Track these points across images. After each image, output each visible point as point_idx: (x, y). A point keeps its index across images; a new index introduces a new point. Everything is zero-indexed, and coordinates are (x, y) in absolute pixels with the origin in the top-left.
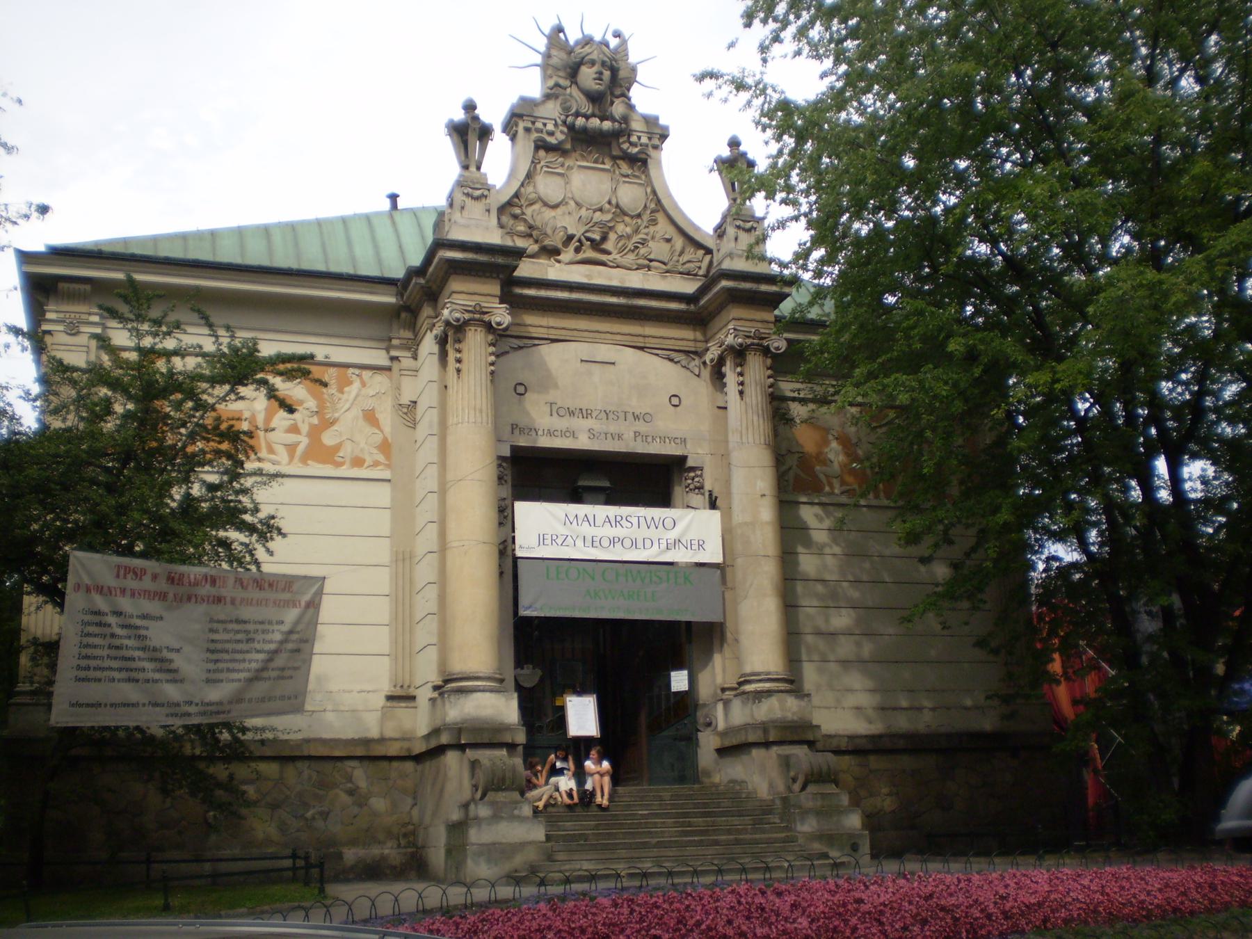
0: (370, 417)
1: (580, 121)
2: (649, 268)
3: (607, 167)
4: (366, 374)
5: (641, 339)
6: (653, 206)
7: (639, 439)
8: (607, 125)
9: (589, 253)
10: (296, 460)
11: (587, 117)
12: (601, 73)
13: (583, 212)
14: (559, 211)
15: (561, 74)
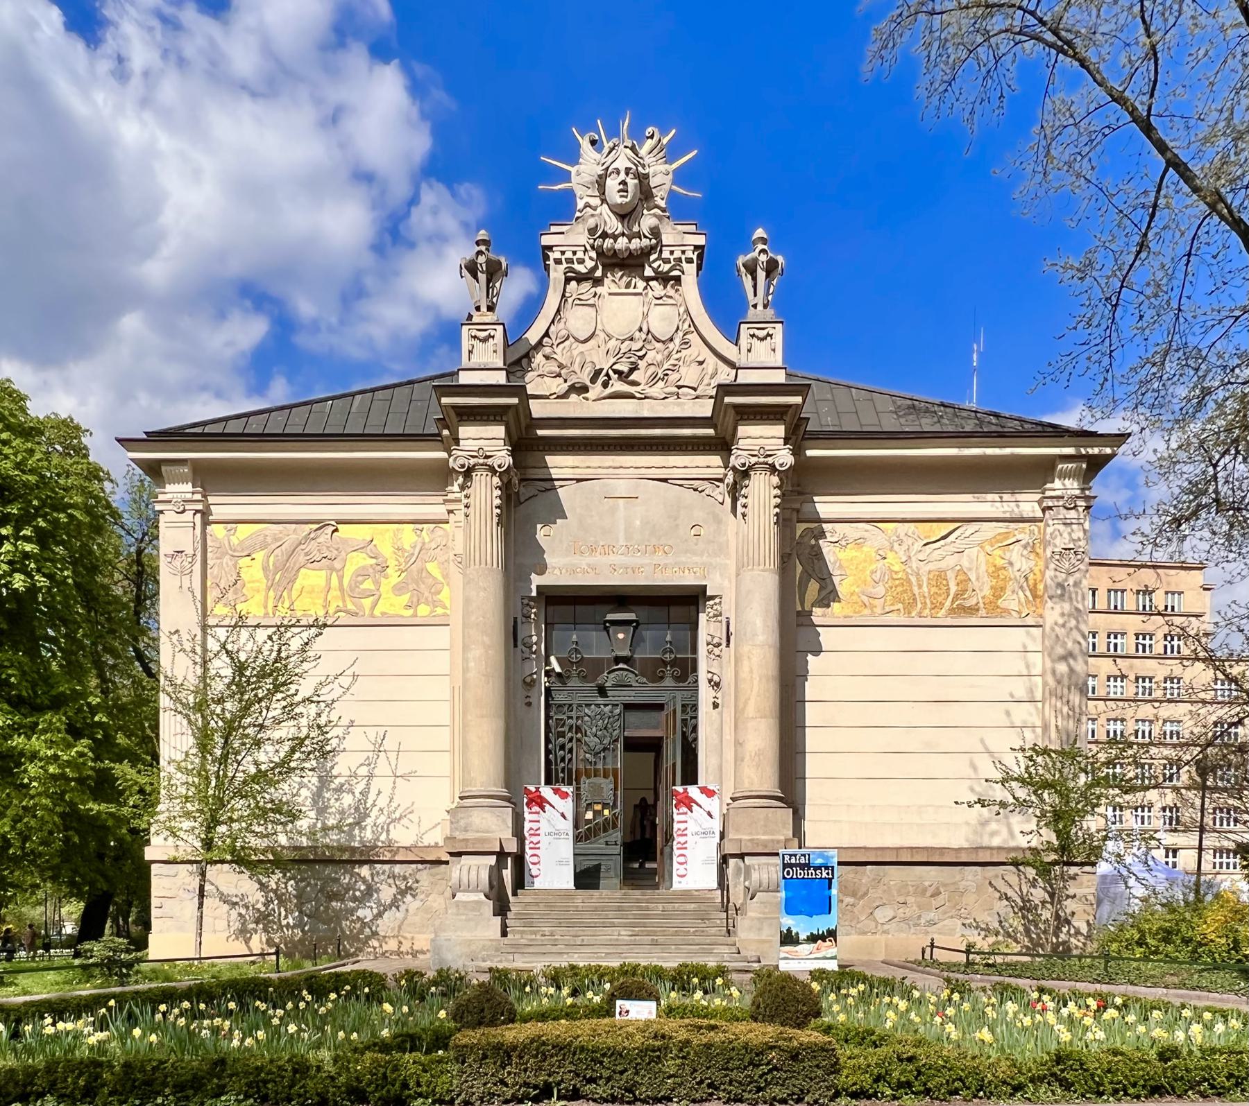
1: (608, 243)
8: (635, 244)
9: (618, 386)
15: (590, 192)
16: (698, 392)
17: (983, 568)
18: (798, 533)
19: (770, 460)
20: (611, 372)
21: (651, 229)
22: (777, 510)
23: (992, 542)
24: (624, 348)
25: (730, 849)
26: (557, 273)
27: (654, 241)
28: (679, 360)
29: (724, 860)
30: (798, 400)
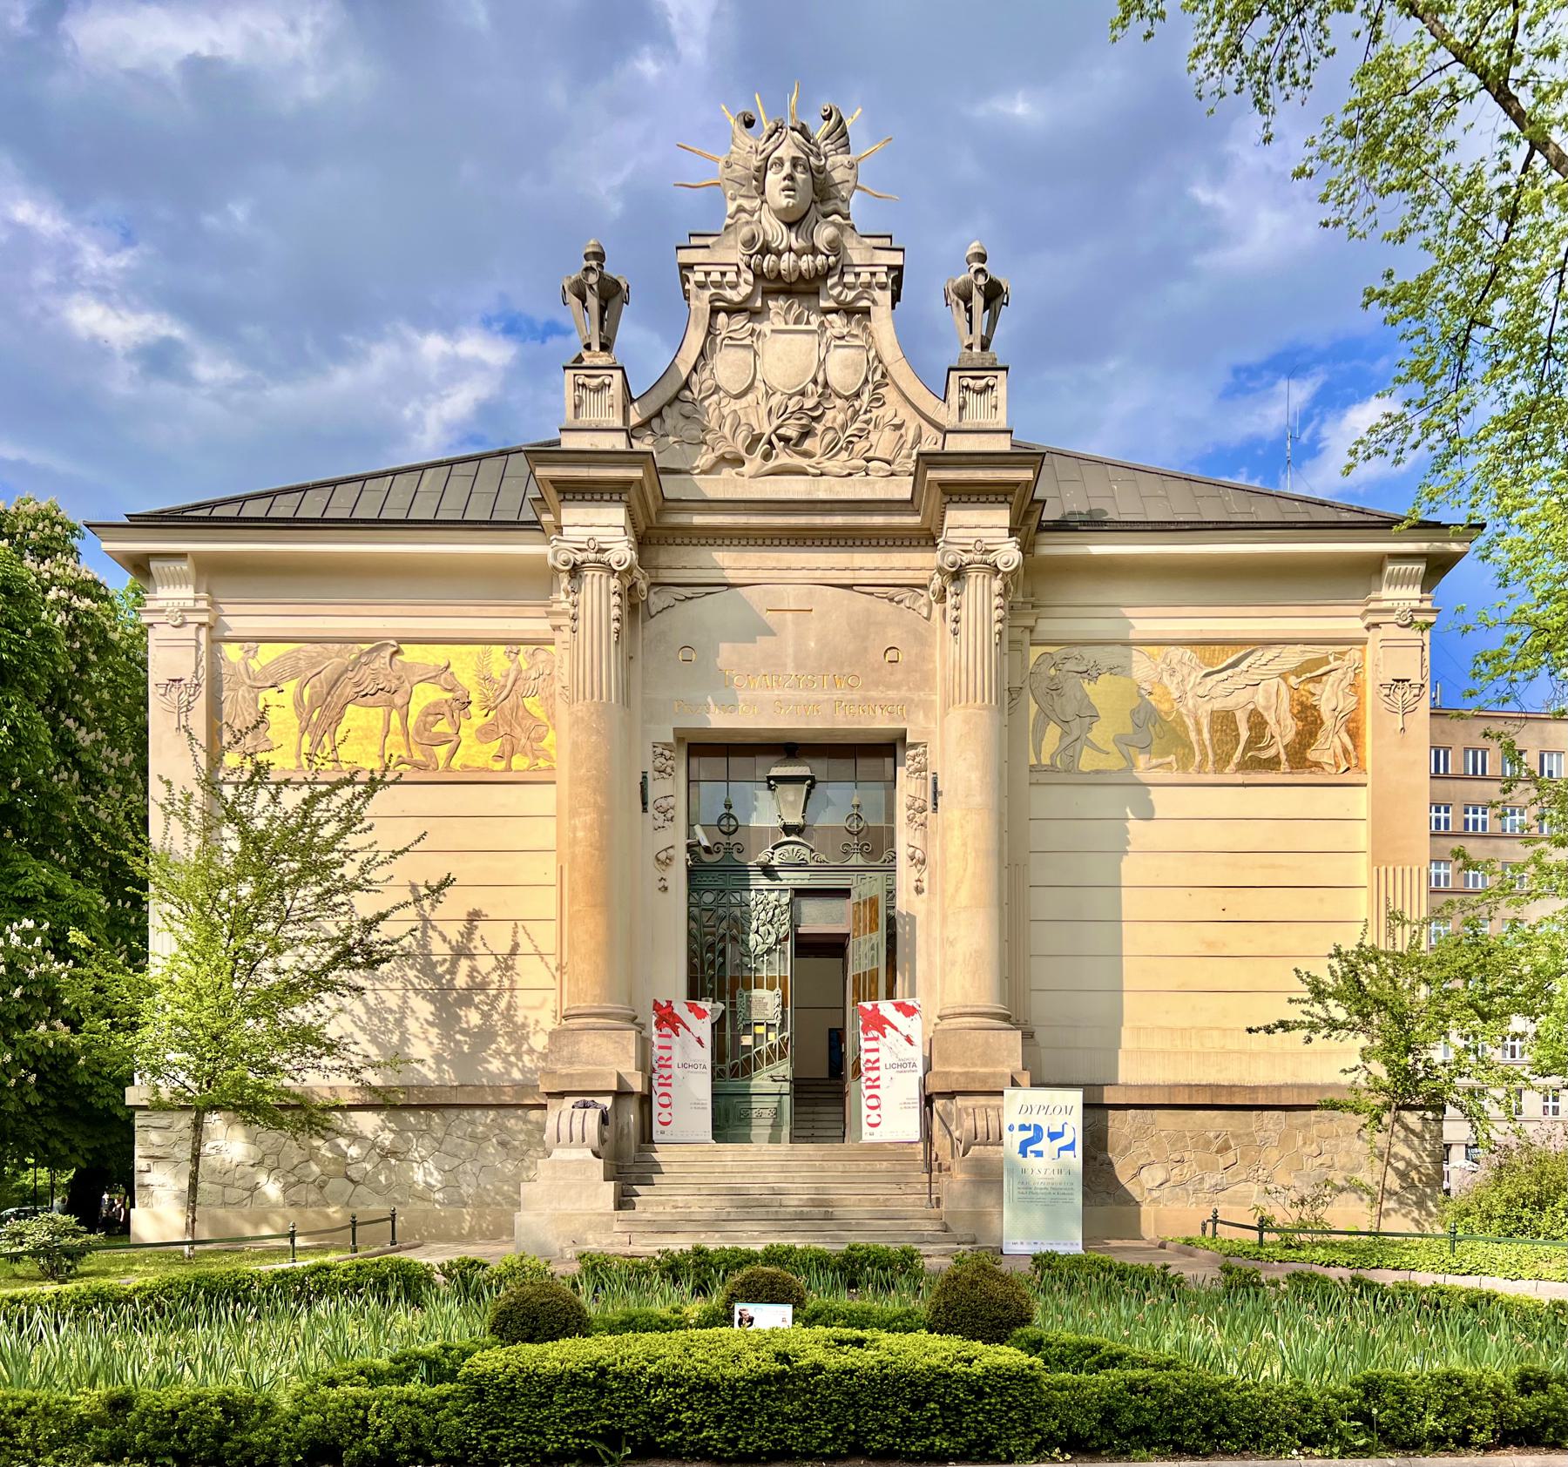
9: (784, 458)
15: (743, 191)
16: (894, 467)
17: (1285, 705)
18: (1032, 660)
19: (990, 558)
20: (774, 438)
21: (829, 243)
22: (999, 626)
23: (1297, 672)
24: (793, 404)
25: (935, 1086)
26: (701, 302)
27: (832, 259)
28: (868, 422)
29: (928, 1100)
30: (1028, 475)
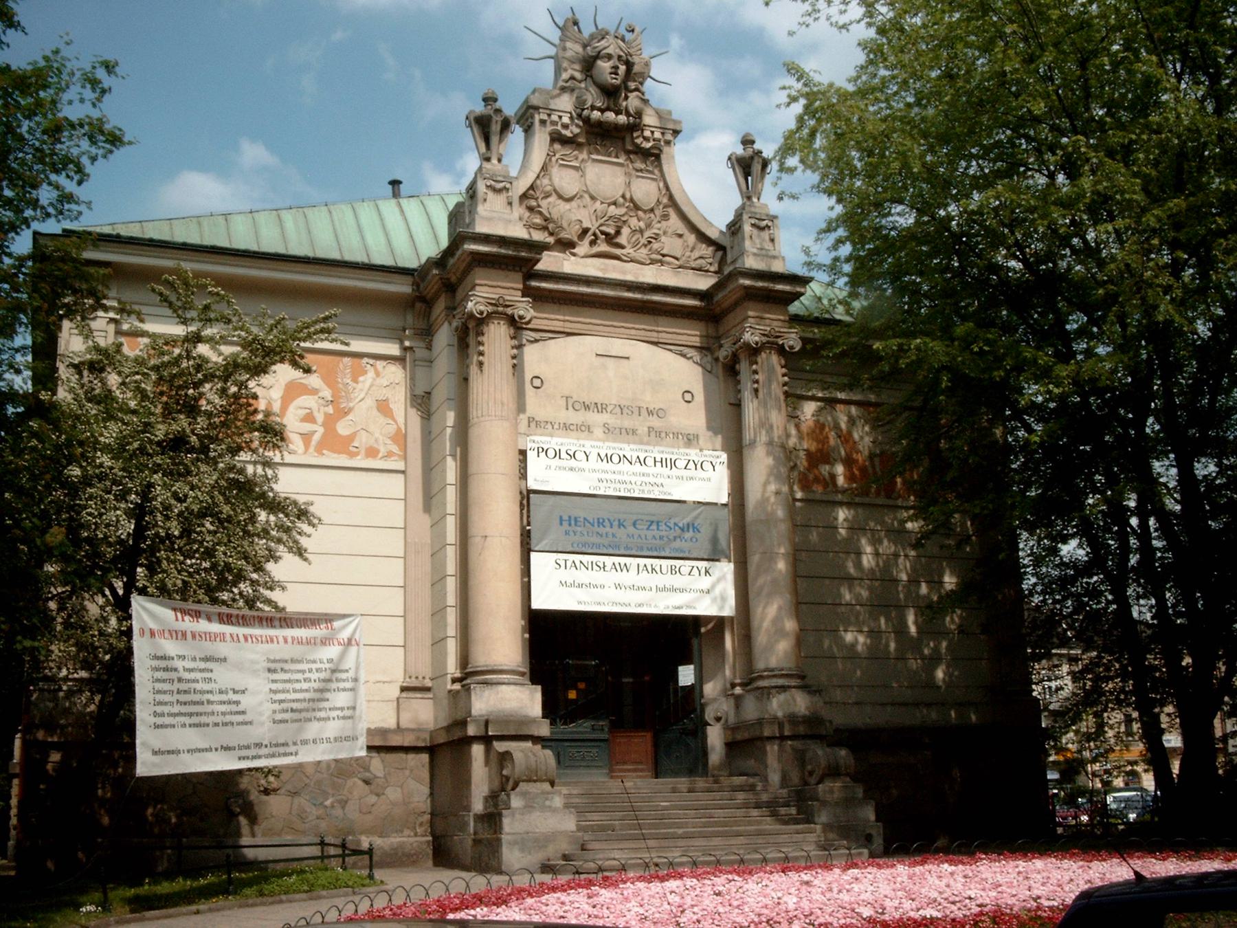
0: (383, 407)
1: (596, 115)
2: (662, 263)
3: (621, 161)
4: (380, 364)
5: (655, 334)
6: (665, 200)
7: (653, 434)
8: (622, 119)
9: (603, 247)
10: (312, 449)
11: (602, 111)
12: (617, 68)
13: (598, 205)
14: (574, 204)
